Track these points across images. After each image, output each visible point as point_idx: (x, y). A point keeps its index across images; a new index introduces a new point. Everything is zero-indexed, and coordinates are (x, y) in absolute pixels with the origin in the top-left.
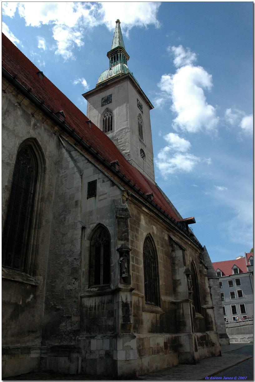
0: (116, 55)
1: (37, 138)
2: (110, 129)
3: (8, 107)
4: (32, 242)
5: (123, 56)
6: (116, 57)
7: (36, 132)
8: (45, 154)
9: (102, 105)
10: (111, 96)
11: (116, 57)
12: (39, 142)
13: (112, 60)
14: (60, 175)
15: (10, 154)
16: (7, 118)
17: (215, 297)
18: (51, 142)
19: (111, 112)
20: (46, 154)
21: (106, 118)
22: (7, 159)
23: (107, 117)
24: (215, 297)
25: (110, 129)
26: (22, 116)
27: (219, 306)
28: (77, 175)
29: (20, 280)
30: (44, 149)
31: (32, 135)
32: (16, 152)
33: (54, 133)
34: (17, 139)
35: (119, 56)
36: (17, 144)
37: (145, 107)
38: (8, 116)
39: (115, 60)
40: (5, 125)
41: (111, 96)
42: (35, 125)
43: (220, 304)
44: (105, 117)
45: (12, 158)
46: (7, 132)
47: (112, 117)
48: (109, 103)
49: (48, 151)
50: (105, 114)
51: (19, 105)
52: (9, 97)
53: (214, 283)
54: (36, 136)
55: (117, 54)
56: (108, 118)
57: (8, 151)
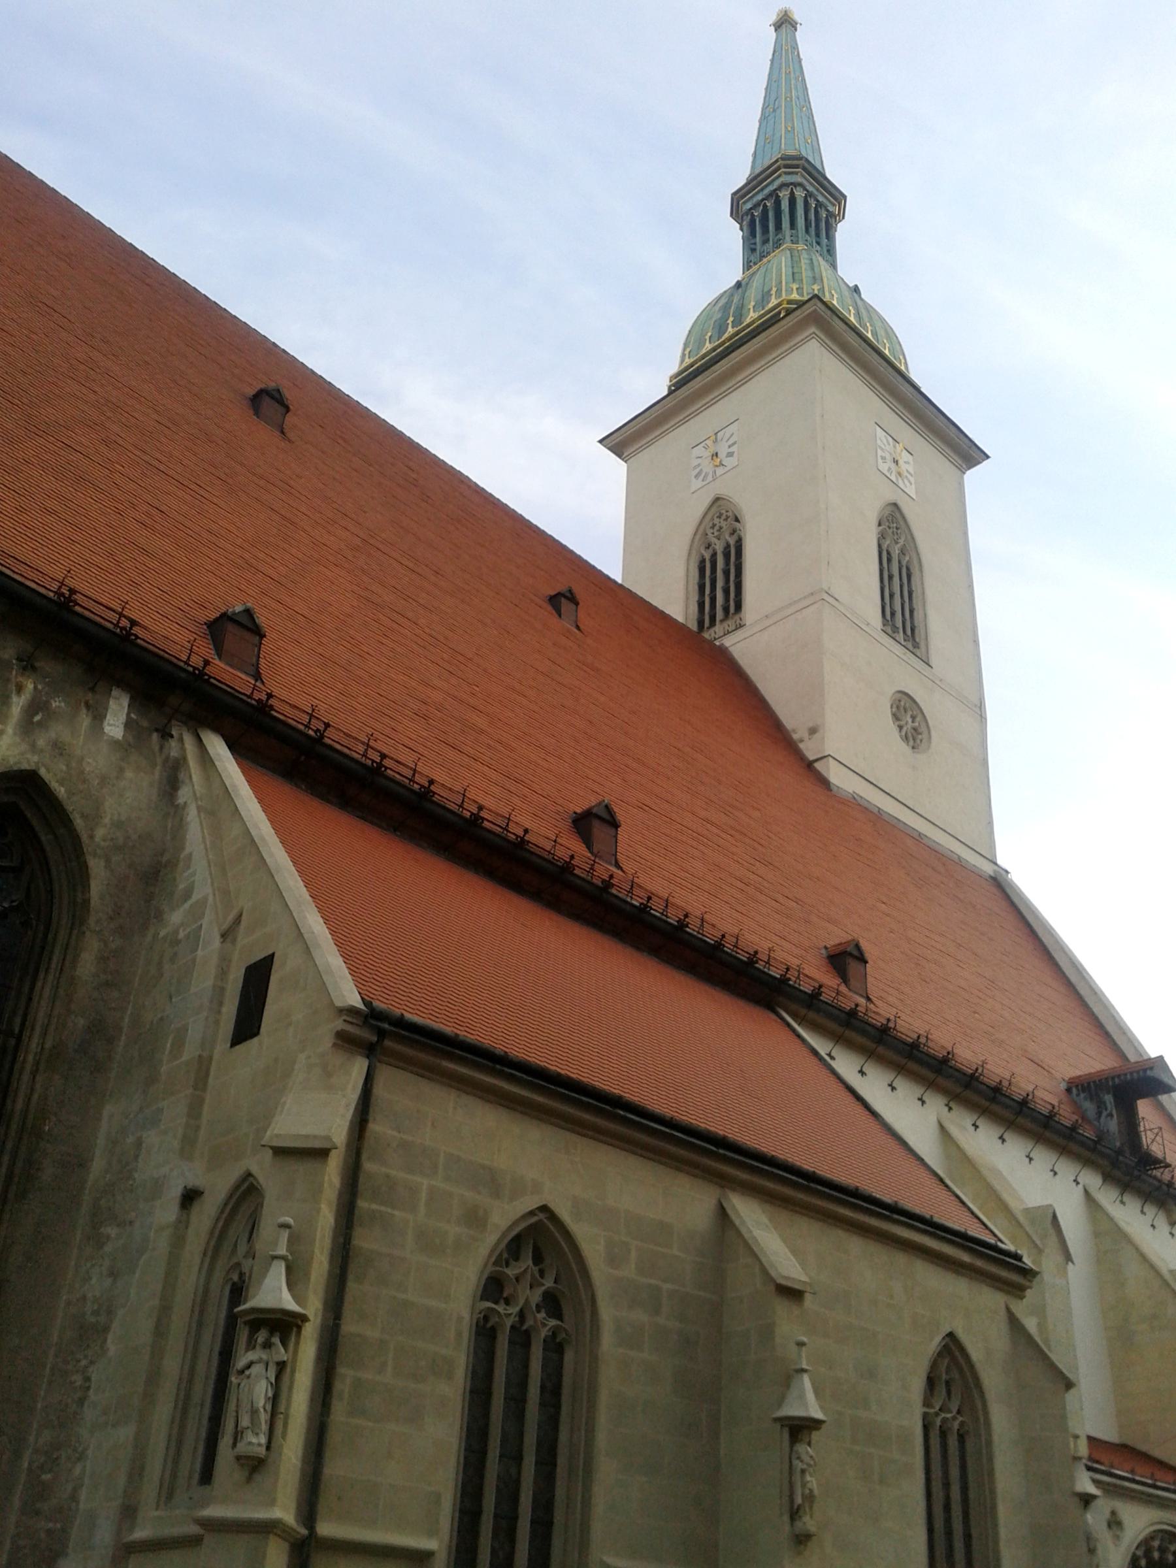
1: (43, 772)
2: (732, 609)
7: (41, 743)
8: (84, 838)
12: (54, 785)
14: (162, 934)
18: (129, 774)
19: (737, 520)
20: (91, 837)
21: (714, 555)
23: (719, 547)
25: (732, 609)
30: (83, 816)
33: (157, 730)
49: (107, 820)
50: (709, 532)
54: (36, 758)
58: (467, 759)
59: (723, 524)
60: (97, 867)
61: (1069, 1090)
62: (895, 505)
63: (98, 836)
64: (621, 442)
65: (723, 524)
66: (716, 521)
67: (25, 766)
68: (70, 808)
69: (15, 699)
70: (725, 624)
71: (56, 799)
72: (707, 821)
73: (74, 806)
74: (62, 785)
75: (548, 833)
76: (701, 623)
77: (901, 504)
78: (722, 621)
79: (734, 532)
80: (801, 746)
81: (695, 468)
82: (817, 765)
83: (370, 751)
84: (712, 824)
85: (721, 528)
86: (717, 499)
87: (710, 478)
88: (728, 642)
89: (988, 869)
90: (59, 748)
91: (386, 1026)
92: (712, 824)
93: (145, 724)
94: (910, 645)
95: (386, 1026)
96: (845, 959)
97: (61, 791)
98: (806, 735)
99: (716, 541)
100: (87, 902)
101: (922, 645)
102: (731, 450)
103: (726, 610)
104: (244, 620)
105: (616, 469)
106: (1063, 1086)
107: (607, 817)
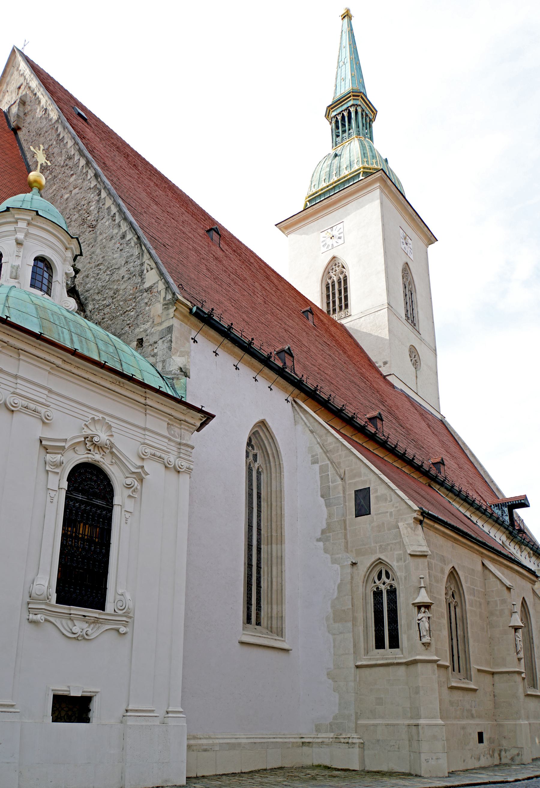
0: (346, 114)
2: (343, 307)
5: (362, 114)
13: (337, 127)
19: (343, 267)
21: (333, 282)
25: (343, 307)
39: (343, 125)
50: (331, 271)
59: (337, 269)
62: (407, 263)
65: (337, 269)
66: (334, 267)
70: (340, 313)
76: (329, 312)
77: (409, 263)
78: (339, 312)
79: (342, 273)
80: (380, 369)
81: (323, 241)
82: (387, 378)
86: (334, 257)
87: (330, 247)
88: (343, 322)
89: (439, 417)
94: (413, 324)
98: (382, 365)
99: (334, 276)
101: (417, 325)
102: (340, 236)
103: (341, 308)
104: (288, 351)
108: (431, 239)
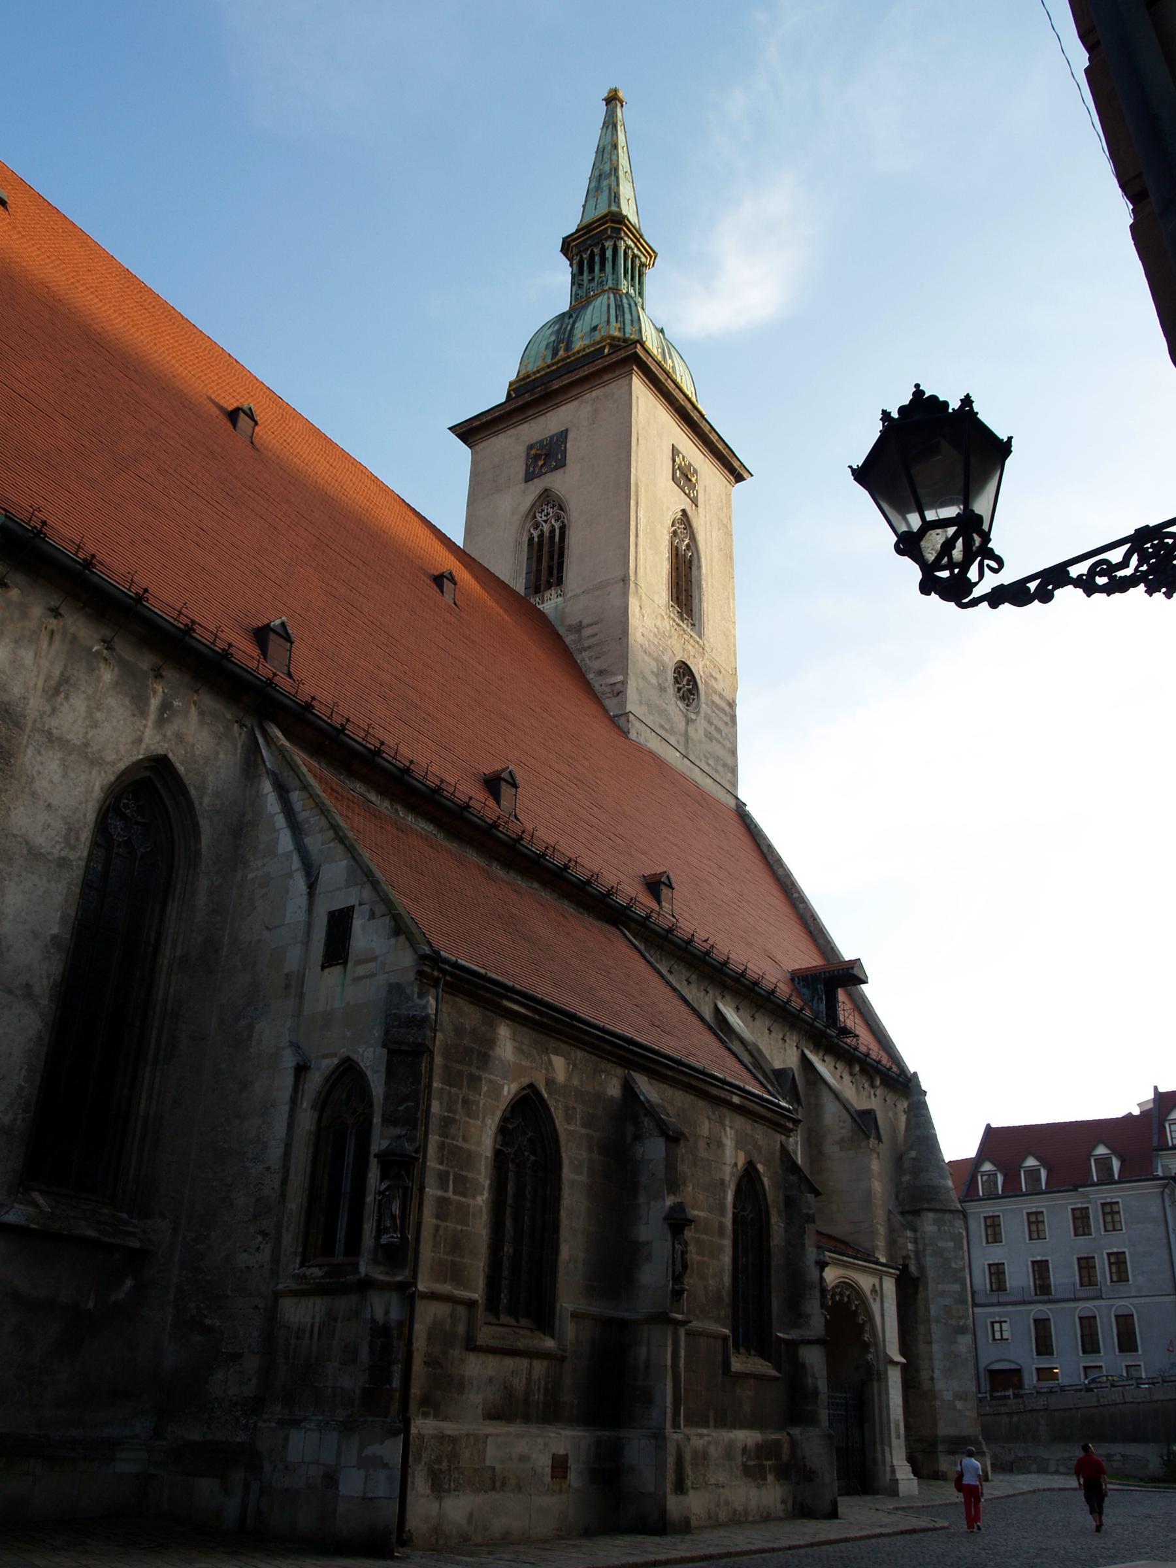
0: (596, 251)
1: (170, 755)
3: (65, 667)
4: (142, 1106)
5: (626, 253)
6: (597, 259)
7: (169, 733)
8: (196, 803)
9: (529, 477)
10: (563, 435)
11: (597, 259)
12: (177, 765)
13: (581, 272)
14: (250, 876)
15: (70, 829)
16: (62, 704)
17: (940, 1287)
19: (561, 509)
20: (201, 803)
22: (58, 847)
24: (940, 1287)
26: (116, 684)
27: (954, 1322)
28: (299, 883)
29: (91, 1233)
31: (153, 747)
32: (91, 817)
34: (94, 772)
35: (609, 253)
36: (97, 788)
37: (708, 472)
38: (67, 698)
40: (54, 731)
41: (563, 435)
42: (165, 707)
43: (960, 1318)
44: (537, 526)
45: (77, 839)
46: (59, 755)
47: (563, 528)
48: (555, 469)
49: (210, 791)
51: (107, 648)
52: (73, 629)
53: (939, 1230)
54: (166, 746)
55: (603, 246)
56: (547, 534)
57: (63, 818)
58: (416, 733)
60: (204, 824)
61: (792, 980)
63: (204, 802)
64: (470, 432)
65: (551, 511)
67: (161, 752)
68: (187, 783)
69: (153, 701)
71: (179, 775)
72: (559, 772)
73: (190, 780)
74: (182, 763)
75: (466, 790)
83: (334, 715)
84: (563, 775)
85: (548, 514)
90: (180, 737)
91: (447, 967)
92: (563, 775)
93: (229, 717)
95: (447, 967)
96: (656, 885)
97: (181, 769)
100: (198, 853)
105: (462, 453)
106: (789, 976)
107: (510, 780)
108: (735, 472)
